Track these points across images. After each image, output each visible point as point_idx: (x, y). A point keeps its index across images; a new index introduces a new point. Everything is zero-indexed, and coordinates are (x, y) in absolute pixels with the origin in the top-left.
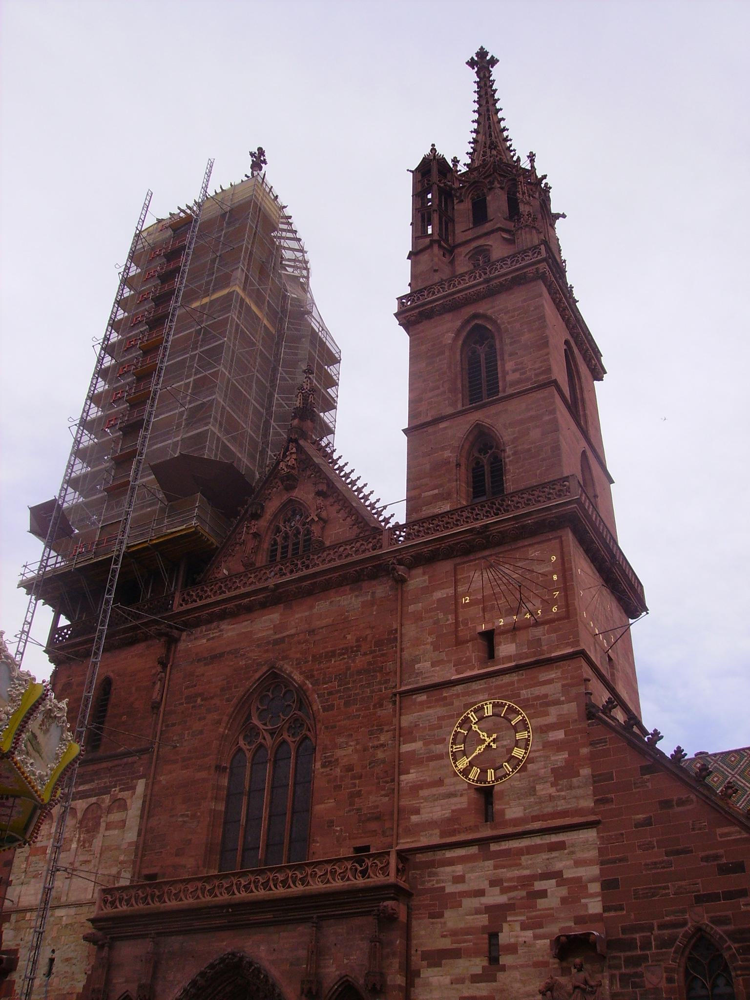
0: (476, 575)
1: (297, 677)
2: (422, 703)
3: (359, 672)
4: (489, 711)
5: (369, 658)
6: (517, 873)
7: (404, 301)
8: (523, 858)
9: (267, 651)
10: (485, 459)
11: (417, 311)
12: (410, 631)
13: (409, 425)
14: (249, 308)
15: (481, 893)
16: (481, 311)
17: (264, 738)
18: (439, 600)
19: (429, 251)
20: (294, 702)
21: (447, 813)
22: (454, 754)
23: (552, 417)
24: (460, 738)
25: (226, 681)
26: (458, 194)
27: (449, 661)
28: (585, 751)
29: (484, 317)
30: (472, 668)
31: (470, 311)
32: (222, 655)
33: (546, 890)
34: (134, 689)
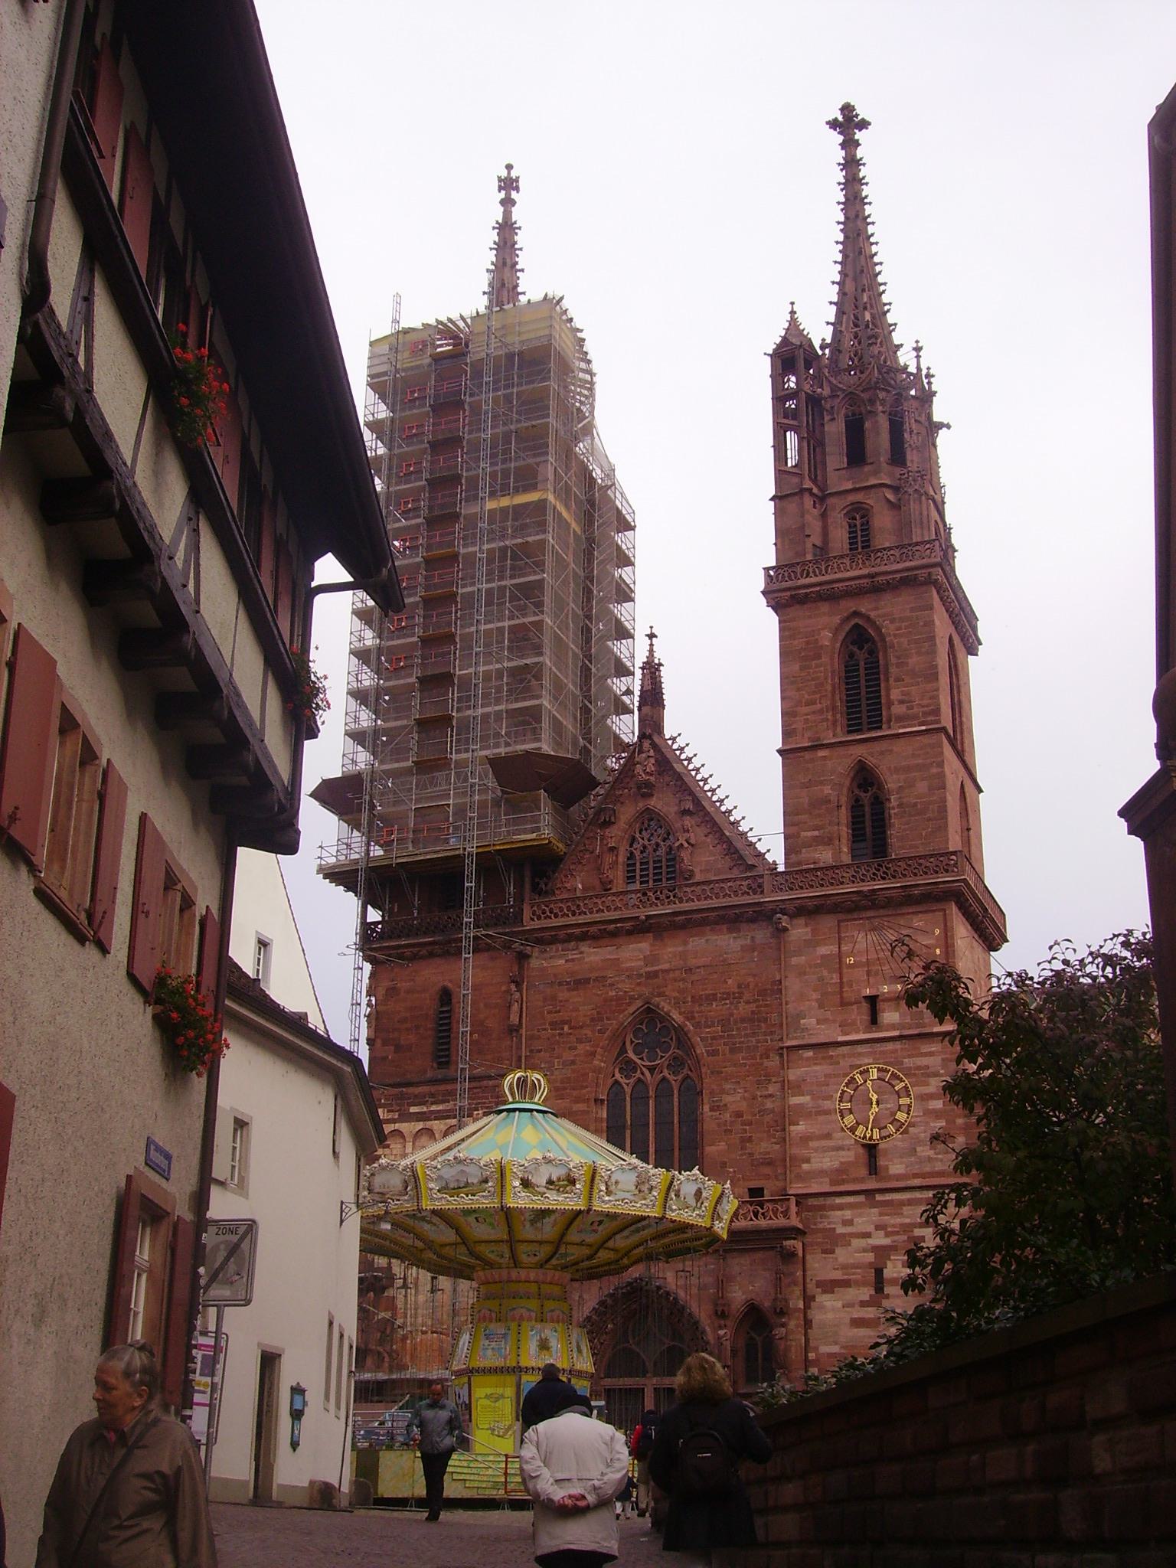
0: (860, 936)
1: (675, 1015)
2: (808, 1059)
3: (743, 1020)
4: (874, 1074)
5: (753, 1006)
6: (899, 1220)
7: (772, 573)
8: (904, 1208)
9: (639, 984)
10: (866, 798)
11: (788, 593)
12: (793, 985)
13: (783, 743)
14: (560, 514)
15: (868, 1235)
16: (863, 610)
17: (642, 1073)
18: (823, 957)
19: (797, 498)
20: (671, 1039)
21: (836, 1164)
22: (841, 1111)
23: (940, 770)
24: (846, 1097)
25: (595, 1012)
26: (828, 406)
27: (834, 1021)
28: (960, 1121)
29: (868, 619)
30: (857, 1032)
31: (850, 605)
32: (587, 981)
33: (923, 1237)
34: (482, 1005)
